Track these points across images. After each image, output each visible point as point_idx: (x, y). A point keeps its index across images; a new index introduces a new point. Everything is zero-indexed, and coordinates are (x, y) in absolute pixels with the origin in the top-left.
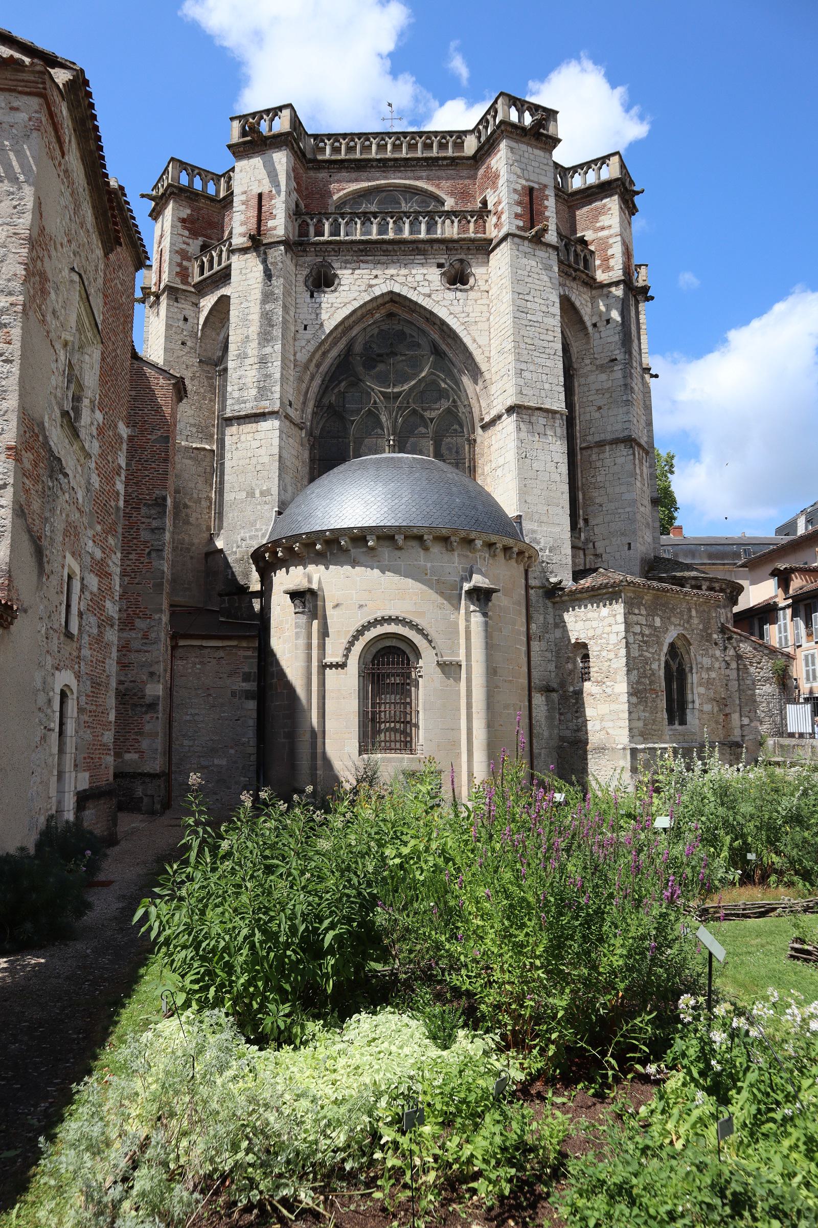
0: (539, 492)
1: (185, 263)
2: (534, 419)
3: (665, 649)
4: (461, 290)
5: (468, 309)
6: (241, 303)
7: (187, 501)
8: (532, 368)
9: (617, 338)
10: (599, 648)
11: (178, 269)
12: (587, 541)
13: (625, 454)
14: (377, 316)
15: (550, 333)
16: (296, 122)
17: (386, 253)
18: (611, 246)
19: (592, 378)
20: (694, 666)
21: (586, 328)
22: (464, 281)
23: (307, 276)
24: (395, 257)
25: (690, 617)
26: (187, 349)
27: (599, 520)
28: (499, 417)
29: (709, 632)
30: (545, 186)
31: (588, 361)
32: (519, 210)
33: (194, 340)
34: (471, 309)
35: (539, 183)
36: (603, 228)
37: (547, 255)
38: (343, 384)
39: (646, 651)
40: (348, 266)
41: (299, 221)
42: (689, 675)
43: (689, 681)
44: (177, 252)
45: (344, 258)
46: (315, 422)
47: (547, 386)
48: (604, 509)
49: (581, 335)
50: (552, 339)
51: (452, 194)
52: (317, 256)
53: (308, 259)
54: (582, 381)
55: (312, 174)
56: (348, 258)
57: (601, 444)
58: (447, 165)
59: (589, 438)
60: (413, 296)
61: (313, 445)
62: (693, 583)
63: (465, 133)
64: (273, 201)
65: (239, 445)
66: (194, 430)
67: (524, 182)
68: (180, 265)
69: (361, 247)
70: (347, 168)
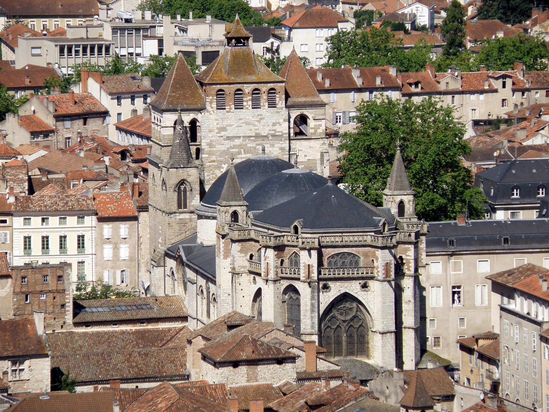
5: (368, 297)
18: (411, 263)
22: (367, 287)
36: (408, 256)
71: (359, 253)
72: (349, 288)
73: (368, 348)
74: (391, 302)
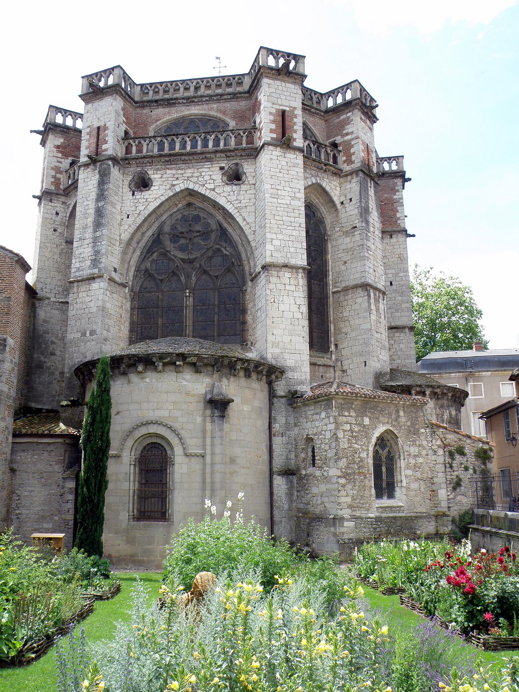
0: (284, 327)
1: (58, 175)
2: (281, 274)
3: (374, 440)
4: (236, 185)
6: (84, 202)
7: (53, 339)
8: (280, 237)
9: (356, 211)
10: (320, 442)
11: (53, 180)
12: (337, 360)
13: (363, 295)
14: (180, 205)
15: (296, 211)
16: (126, 77)
17: (184, 162)
19: (340, 241)
20: (402, 455)
21: (335, 206)
23: (131, 181)
24: (191, 165)
25: (399, 416)
26: (57, 234)
27: (345, 345)
28: (259, 273)
29: (417, 427)
30: (295, 108)
31: (337, 229)
32: (273, 126)
33: (63, 228)
34: (243, 197)
35: (289, 107)
36: (347, 134)
37: (295, 156)
38: (155, 254)
39: (355, 443)
40: (158, 172)
41: (126, 144)
42: (398, 460)
43: (398, 465)
44: (52, 169)
45: (156, 167)
46: (135, 282)
47: (292, 250)
48: (348, 336)
49: (333, 210)
50: (297, 215)
51: (234, 118)
52: (137, 167)
53: (131, 169)
54: (334, 243)
55: (139, 110)
56: (158, 167)
57: (346, 289)
58: (207, 101)
59: (339, 284)
60: (202, 191)
61: (134, 298)
62: (418, 389)
63: (243, 75)
64: (107, 132)
65: (77, 300)
66: (61, 289)
67: (278, 107)
68: (54, 177)
69: (167, 159)
70: (162, 105)
71: (224, 113)
72: (194, 179)
73: (244, 323)
74: (293, 198)
